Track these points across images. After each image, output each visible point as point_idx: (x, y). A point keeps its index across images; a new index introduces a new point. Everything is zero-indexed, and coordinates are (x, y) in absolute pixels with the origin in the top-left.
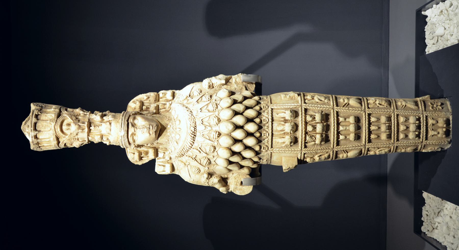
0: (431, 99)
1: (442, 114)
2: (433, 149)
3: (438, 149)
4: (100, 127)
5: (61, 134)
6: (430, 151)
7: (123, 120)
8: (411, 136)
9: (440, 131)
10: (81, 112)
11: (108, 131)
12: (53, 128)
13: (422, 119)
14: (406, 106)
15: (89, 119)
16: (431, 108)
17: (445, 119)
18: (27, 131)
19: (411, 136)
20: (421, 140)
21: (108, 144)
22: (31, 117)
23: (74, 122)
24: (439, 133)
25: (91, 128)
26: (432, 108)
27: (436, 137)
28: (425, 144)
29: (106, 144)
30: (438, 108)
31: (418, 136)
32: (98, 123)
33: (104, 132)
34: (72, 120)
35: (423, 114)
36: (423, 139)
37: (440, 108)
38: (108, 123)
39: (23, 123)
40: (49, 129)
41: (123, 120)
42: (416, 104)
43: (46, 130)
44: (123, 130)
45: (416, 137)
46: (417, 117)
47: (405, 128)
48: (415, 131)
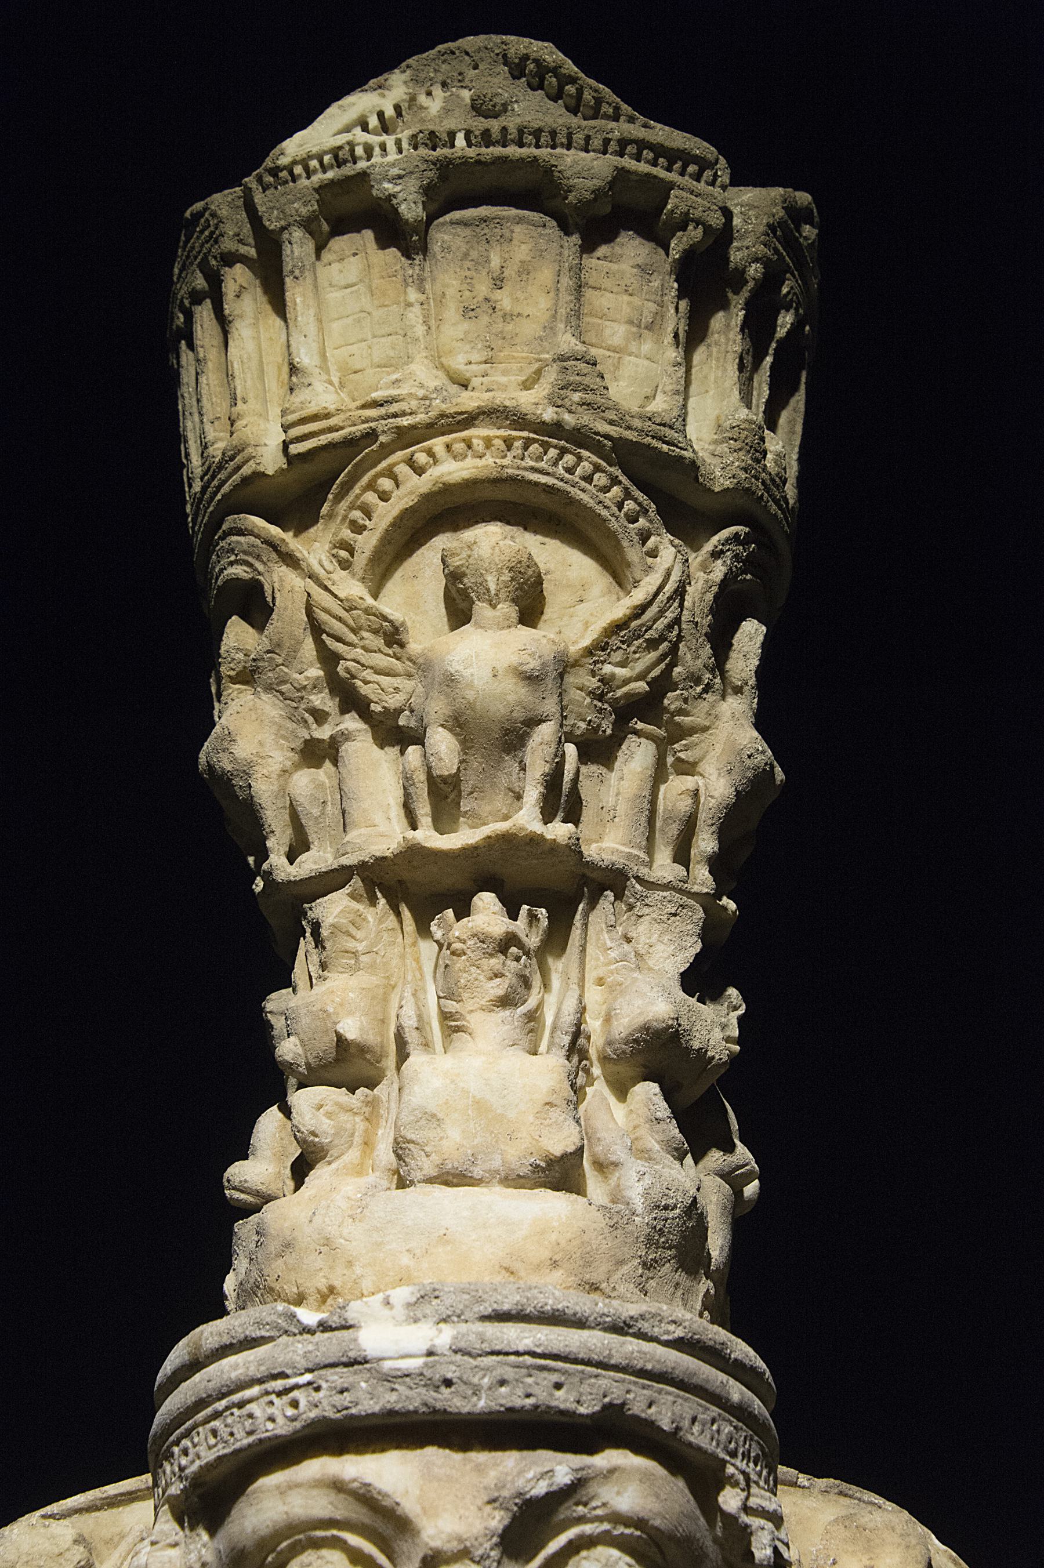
4: (491, 1029)
5: (386, 514)
7: (629, 1348)
10: (716, 785)
11: (452, 1142)
12: (469, 401)
15: (612, 881)
18: (434, 104)
21: (254, 1172)
22: (621, 129)
23: (564, 666)
25: (487, 907)
29: (242, 1151)
32: (556, 1004)
33: (431, 1077)
34: (600, 647)
38: (560, 1141)
39: (547, 52)
40: (458, 362)
41: (629, 1348)
43: (454, 328)
44: (444, 1337)
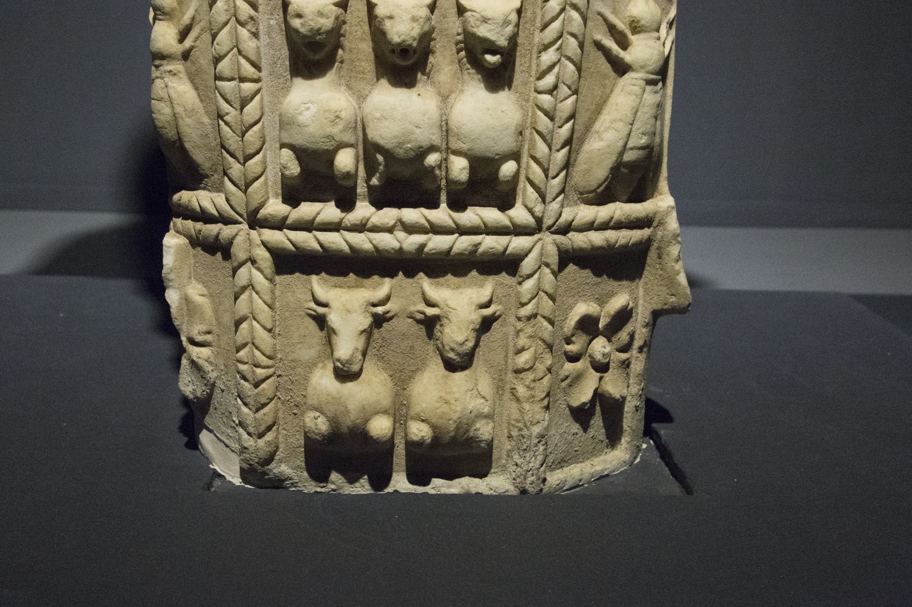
0: (656, 315)
1: (534, 411)
2: (196, 330)
3: (194, 364)
6: (172, 296)
8: (318, 105)
9: (372, 388)
13: (492, 215)
14: (621, 68)
16: (582, 309)
17: (484, 430)
19: (318, 105)
20: (275, 207)
24: (345, 374)
26: (588, 325)
27: (307, 353)
28: (239, 251)
30: (578, 378)
31: (314, 177)
35: (537, 228)
36: (280, 224)
37: (583, 395)
42: (631, 178)
45: (301, 153)
46: (508, 169)
47: (402, 30)
48: (370, 151)
